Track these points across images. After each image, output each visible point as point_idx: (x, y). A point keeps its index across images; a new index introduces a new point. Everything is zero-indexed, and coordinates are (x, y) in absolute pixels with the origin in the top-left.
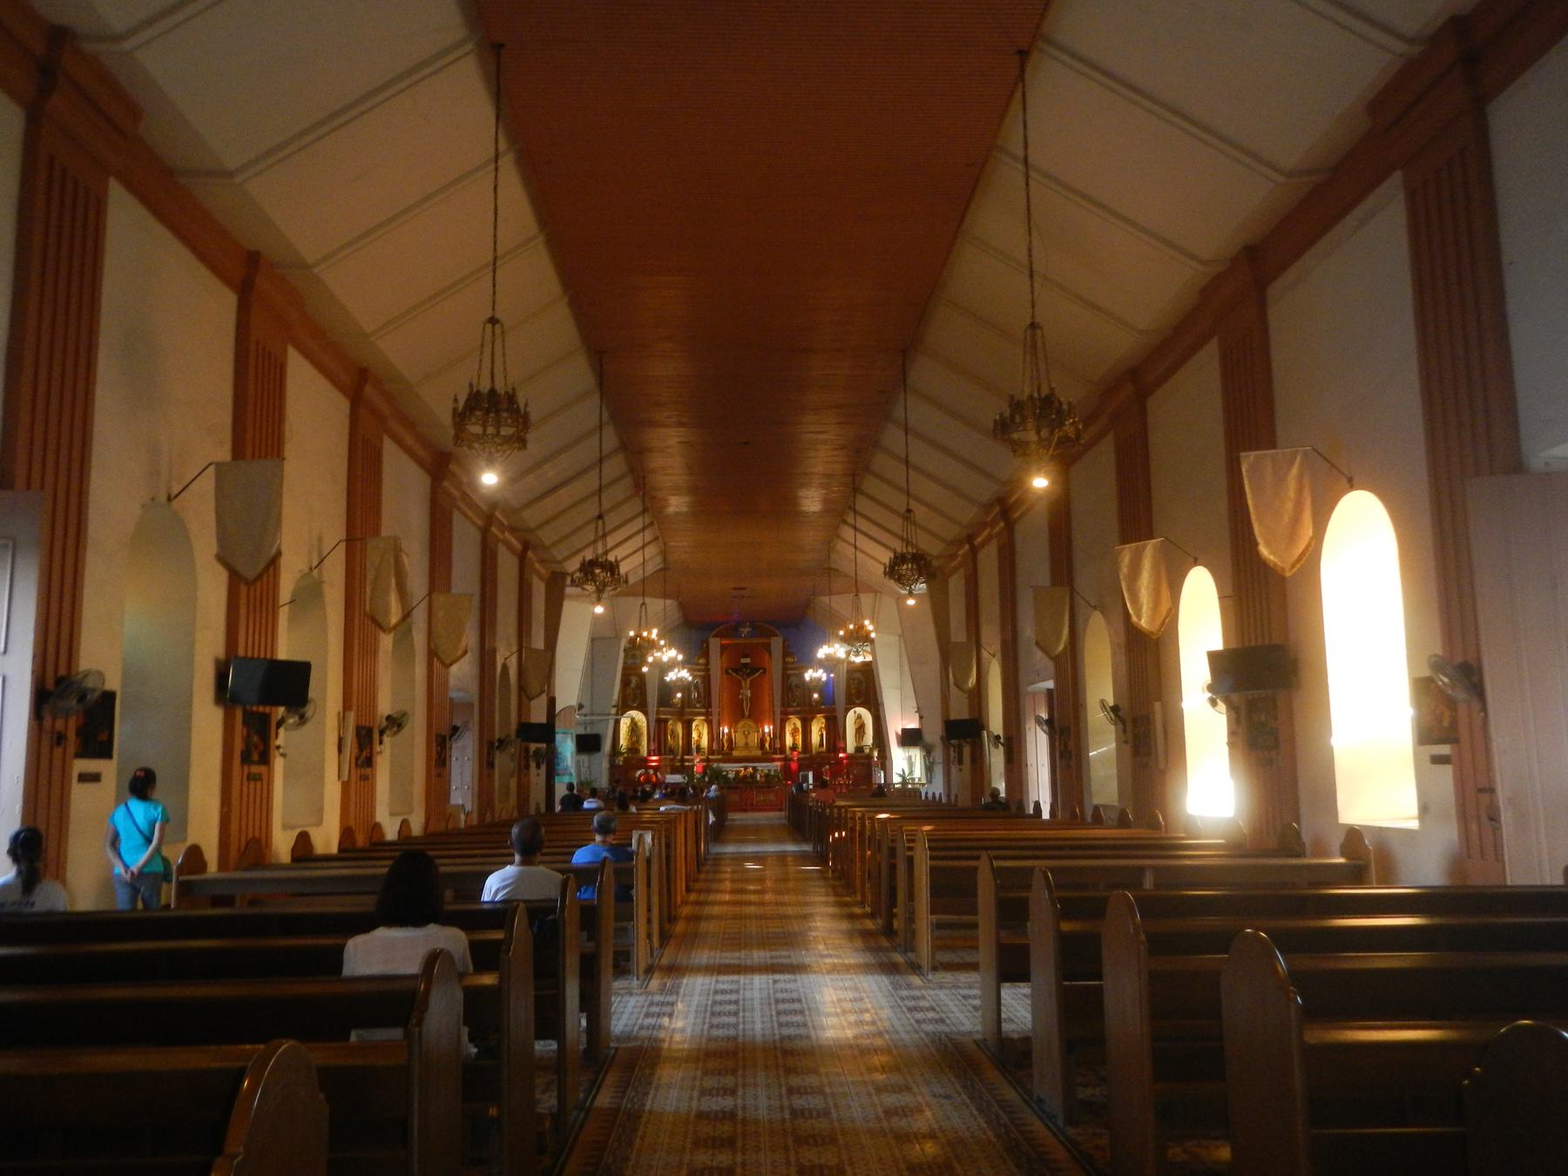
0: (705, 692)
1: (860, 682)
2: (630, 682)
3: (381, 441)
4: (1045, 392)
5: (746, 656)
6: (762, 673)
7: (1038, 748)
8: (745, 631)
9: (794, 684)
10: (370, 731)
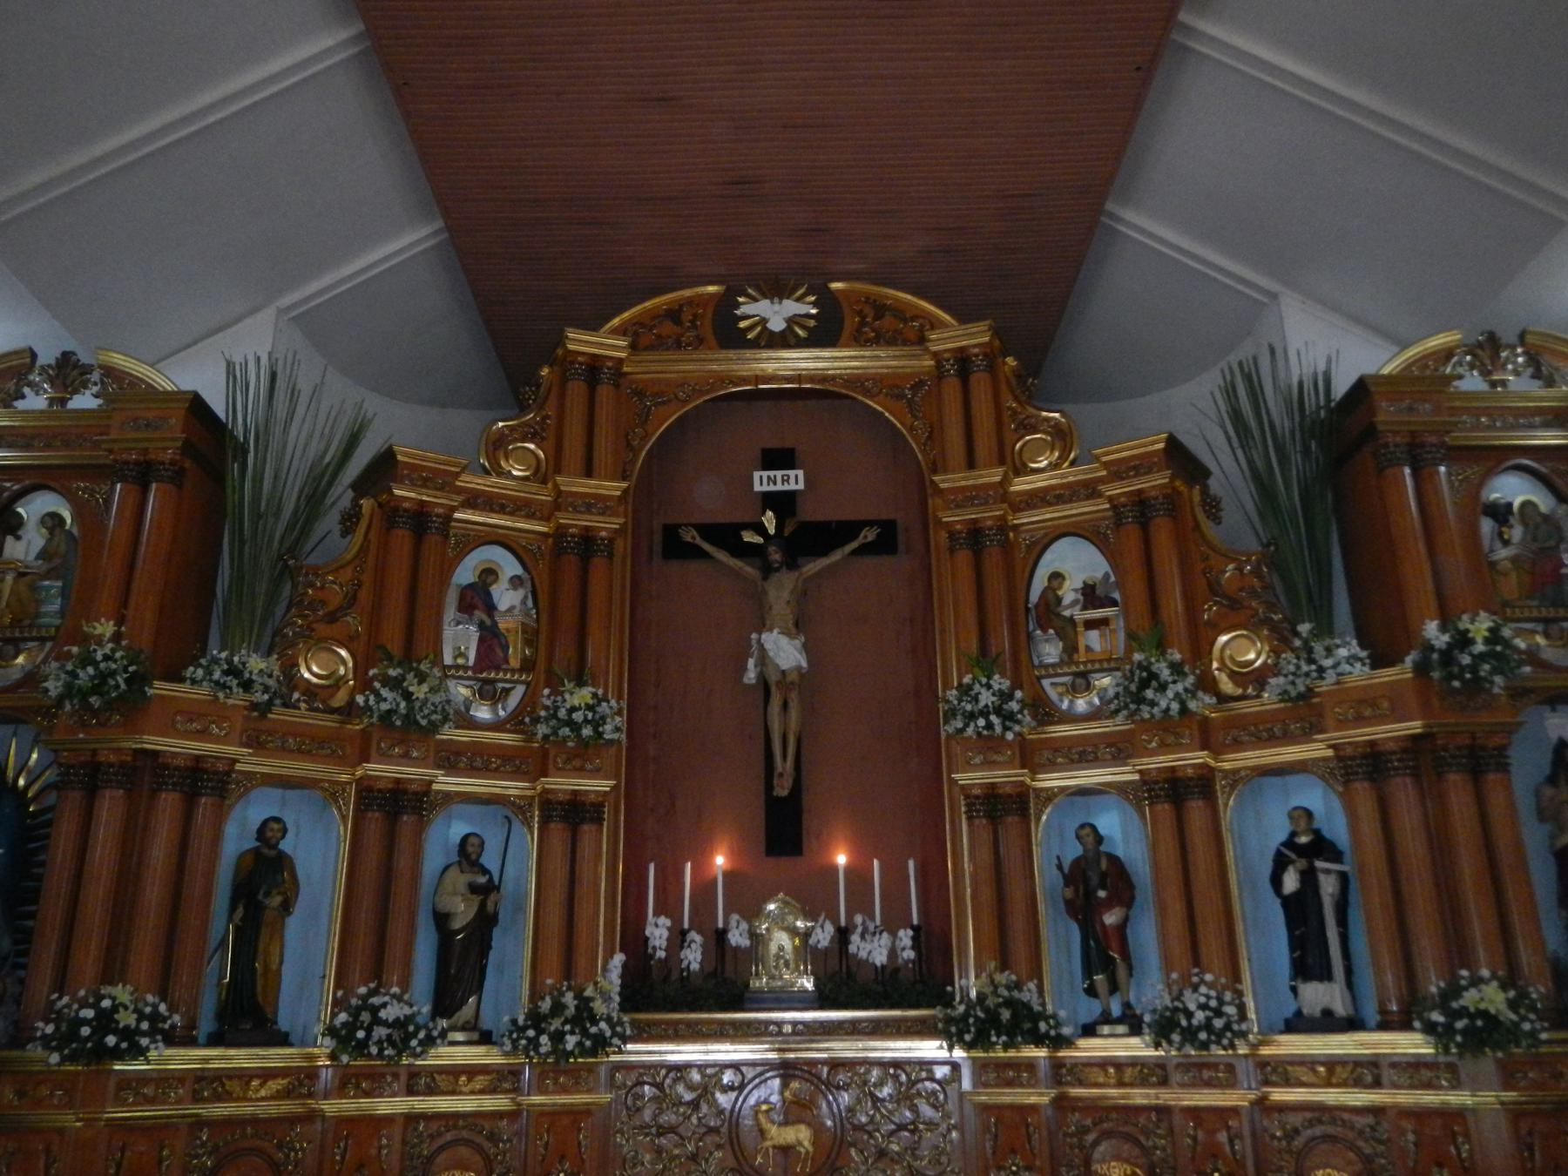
5: (778, 459)
6: (864, 550)
9: (1069, 593)
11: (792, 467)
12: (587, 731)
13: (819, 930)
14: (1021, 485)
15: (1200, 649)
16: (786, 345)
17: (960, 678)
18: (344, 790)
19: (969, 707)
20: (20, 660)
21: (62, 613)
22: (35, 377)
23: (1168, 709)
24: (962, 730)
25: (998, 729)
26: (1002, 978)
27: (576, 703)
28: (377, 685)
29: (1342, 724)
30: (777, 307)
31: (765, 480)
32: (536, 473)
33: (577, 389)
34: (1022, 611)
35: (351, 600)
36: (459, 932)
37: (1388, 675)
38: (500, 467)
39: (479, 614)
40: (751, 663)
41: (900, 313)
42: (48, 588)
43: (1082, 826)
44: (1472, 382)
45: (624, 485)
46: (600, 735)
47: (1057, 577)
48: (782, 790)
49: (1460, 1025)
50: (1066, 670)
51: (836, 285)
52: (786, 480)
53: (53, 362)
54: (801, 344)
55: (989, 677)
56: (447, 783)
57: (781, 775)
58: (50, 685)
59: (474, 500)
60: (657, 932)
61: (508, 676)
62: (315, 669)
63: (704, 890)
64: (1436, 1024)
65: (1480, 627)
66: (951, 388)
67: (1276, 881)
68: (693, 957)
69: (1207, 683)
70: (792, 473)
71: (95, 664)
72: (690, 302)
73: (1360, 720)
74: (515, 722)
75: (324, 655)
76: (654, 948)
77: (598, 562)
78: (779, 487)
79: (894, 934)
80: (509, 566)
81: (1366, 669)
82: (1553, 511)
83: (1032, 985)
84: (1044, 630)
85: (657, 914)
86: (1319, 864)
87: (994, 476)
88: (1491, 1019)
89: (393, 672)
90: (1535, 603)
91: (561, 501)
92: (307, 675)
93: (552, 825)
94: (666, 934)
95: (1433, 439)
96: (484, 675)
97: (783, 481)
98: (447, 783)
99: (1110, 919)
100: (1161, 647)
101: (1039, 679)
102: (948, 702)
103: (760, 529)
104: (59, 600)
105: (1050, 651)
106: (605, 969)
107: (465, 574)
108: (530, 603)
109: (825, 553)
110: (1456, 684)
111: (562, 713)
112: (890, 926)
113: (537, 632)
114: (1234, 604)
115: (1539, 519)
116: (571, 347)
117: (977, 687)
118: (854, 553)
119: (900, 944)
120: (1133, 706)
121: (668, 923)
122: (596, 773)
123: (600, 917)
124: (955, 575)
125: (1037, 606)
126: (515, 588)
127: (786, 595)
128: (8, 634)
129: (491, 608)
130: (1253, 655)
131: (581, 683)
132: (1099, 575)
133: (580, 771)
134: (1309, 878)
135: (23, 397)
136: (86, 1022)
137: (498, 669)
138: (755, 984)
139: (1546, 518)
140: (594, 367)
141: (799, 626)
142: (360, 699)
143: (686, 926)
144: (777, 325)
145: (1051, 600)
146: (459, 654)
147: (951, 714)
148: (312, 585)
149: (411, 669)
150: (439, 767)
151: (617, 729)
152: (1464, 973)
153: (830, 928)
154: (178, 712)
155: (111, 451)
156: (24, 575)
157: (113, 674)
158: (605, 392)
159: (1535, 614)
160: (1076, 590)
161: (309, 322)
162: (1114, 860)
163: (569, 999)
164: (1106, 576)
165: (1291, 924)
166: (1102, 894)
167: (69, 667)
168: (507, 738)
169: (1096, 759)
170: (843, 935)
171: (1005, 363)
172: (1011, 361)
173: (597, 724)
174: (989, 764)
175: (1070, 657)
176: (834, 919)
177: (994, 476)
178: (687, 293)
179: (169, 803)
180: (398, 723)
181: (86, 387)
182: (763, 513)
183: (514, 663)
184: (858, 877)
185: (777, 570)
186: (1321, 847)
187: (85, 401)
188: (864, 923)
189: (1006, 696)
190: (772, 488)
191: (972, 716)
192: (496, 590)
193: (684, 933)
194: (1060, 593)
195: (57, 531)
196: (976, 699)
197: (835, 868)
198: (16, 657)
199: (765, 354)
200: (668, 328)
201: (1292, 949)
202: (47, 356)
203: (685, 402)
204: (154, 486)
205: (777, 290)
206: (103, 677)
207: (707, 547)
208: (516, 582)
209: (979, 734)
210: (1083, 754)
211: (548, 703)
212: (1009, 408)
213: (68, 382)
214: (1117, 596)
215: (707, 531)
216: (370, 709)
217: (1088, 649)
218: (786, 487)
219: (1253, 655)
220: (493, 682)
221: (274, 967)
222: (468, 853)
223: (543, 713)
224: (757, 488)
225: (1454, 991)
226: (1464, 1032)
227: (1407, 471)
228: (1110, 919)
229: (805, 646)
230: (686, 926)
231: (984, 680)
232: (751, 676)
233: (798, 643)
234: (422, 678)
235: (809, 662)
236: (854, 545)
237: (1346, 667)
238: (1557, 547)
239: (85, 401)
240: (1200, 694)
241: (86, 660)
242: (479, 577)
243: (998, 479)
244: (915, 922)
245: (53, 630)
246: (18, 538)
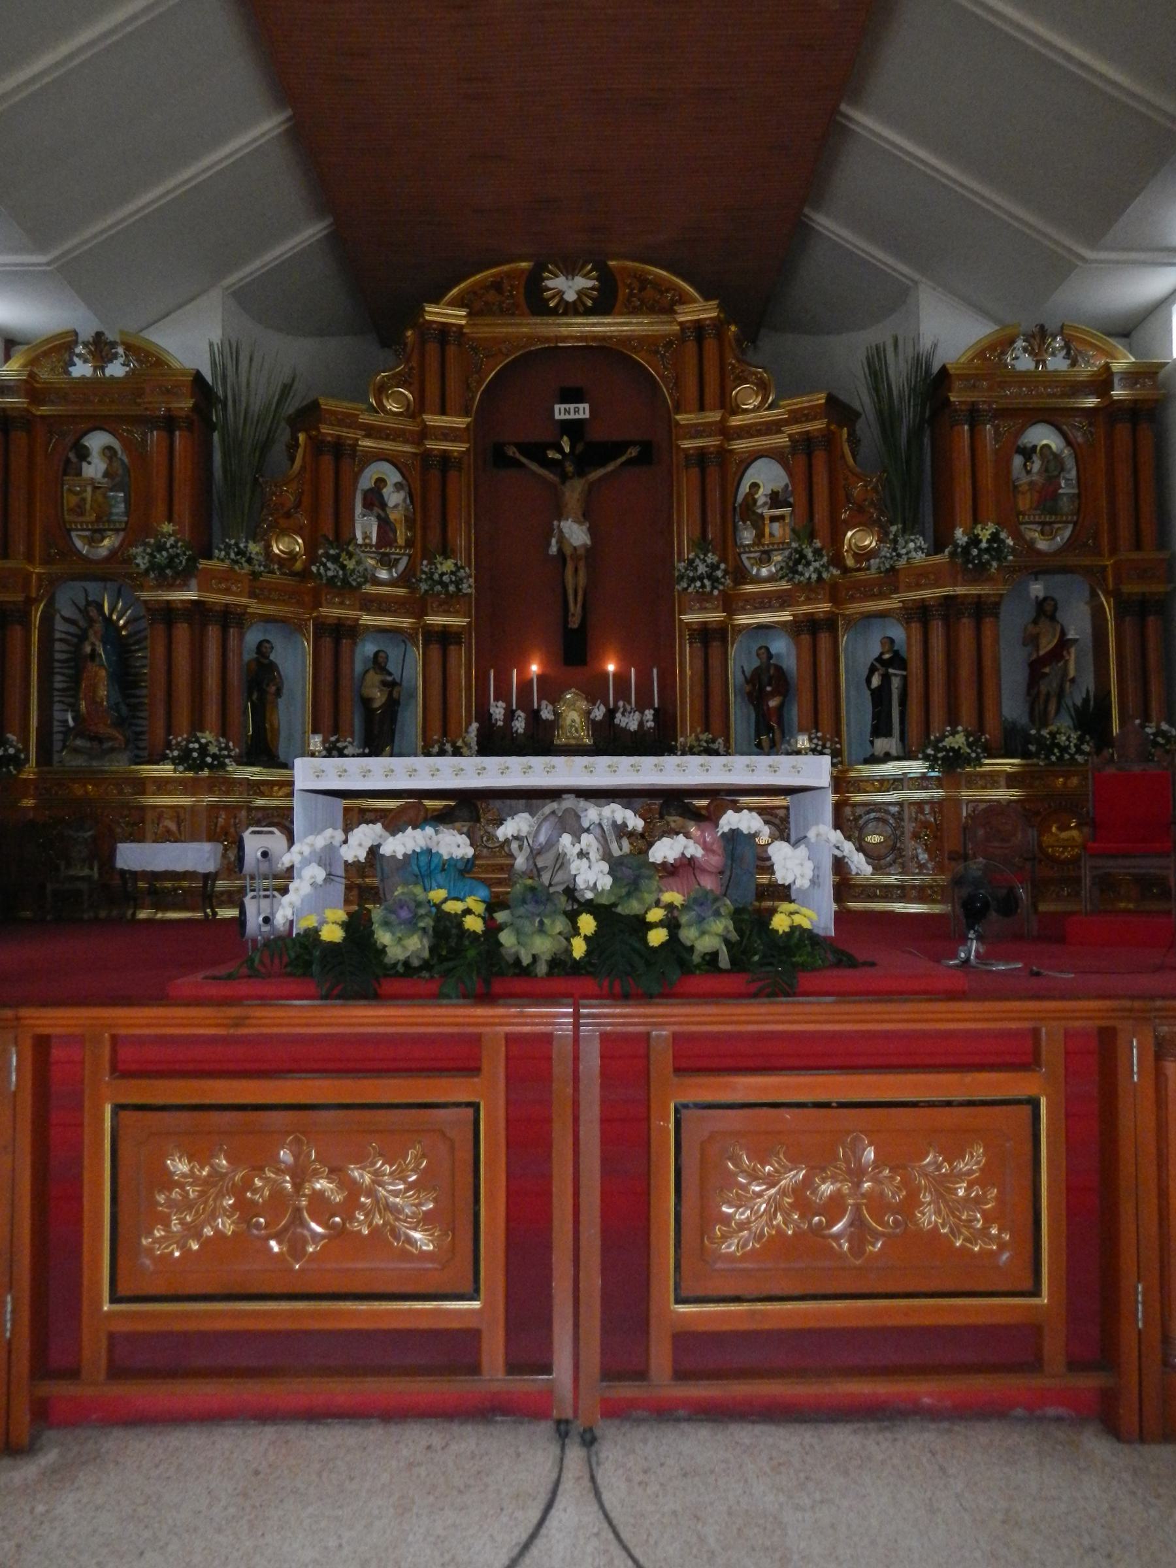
0: (410, 523)
2: (83, 454)
5: (572, 395)
6: (630, 462)
9: (761, 496)
11: (581, 402)
12: (452, 588)
13: (596, 710)
14: (736, 421)
15: (836, 538)
16: (577, 313)
17: (688, 554)
18: (306, 624)
19: (691, 574)
20: (106, 542)
21: (127, 513)
22: (80, 349)
23: (810, 578)
24: (686, 589)
25: (708, 589)
26: (704, 737)
27: (445, 570)
28: (324, 560)
29: (909, 588)
30: (570, 283)
31: (562, 411)
32: (407, 410)
33: (432, 348)
34: (730, 508)
35: (298, 504)
36: (378, 709)
37: (937, 559)
38: (384, 407)
39: (377, 510)
40: (554, 541)
41: (659, 286)
42: (114, 497)
43: (760, 648)
44: (1025, 363)
45: (469, 420)
46: (459, 590)
47: (755, 486)
48: (574, 623)
49: (940, 755)
50: (756, 548)
51: (612, 263)
52: (577, 411)
53: (91, 340)
54: (589, 312)
55: (705, 555)
56: (368, 619)
57: (573, 615)
58: (139, 561)
59: (371, 432)
60: (497, 711)
61: (398, 551)
62: (281, 547)
63: (525, 686)
64: (930, 755)
65: (985, 534)
66: (691, 347)
67: (868, 681)
68: (519, 725)
69: (837, 560)
70: (581, 406)
71: (167, 550)
72: (508, 275)
73: (919, 586)
74: (404, 580)
75: (286, 539)
76: (496, 720)
77: (453, 474)
78: (572, 416)
79: (642, 713)
80: (393, 476)
81: (923, 556)
82: (1062, 452)
83: (720, 740)
84: (744, 522)
85: (496, 699)
86: (891, 671)
87: (714, 416)
88: (957, 752)
89: (332, 552)
90: (1039, 512)
91: (425, 432)
92: (277, 551)
93: (431, 646)
94: (503, 711)
95: (985, 407)
96: (383, 550)
97: (575, 412)
98: (368, 619)
99: (773, 703)
100: (812, 536)
101: (739, 554)
102: (679, 570)
103: (560, 450)
104: (123, 505)
105: (747, 536)
106: (467, 732)
107: (366, 481)
108: (408, 501)
109: (603, 464)
110: (970, 566)
111: (436, 577)
112: (641, 709)
113: (414, 521)
114: (860, 510)
115: (1051, 457)
116: (428, 318)
117: (697, 560)
118: (623, 464)
119: (645, 718)
120: (790, 575)
121: (504, 705)
122: (456, 614)
123: (462, 703)
124: (687, 484)
125: (740, 505)
126: (398, 491)
127: (576, 496)
128: (96, 527)
129: (383, 505)
130: (870, 541)
131: (446, 558)
132: (782, 484)
133: (447, 613)
134: (886, 678)
135: (75, 365)
136: (194, 750)
137: (390, 545)
138: (557, 742)
139: (1057, 457)
140: (444, 330)
141: (587, 515)
142: (314, 569)
143: (514, 707)
144: (571, 296)
145: (750, 499)
146: (366, 536)
147: (681, 577)
148: (274, 494)
149: (343, 550)
150: (361, 610)
151: (470, 586)
152: (948, 728)
153: (603, 709)
154: (214, 578)
155: (146, 409)
156: (99, 488)
157: (177, 555)
158: (452, 350)
159: (1037, 519)
160: (766, 495)
161: (242, 297)
162: (779, 669)
163: (448, 747)
164: (787, 486)
165: (875, 705)
166: (769, 689)
167: (149, 550)
168: (400, 591)
169: (770, 606)
170: (611, 713)
171: (729, 329)
172: (733, 328)
173: (458, 583)
174: (703, 609)
175: (759, 540)
176: (606, 704)
177: (714, 416)
178: (505, 268)
179: (213, 632)
180: (339, 584)
181: (116, 358)
182: (562, 438)
183: (401, 541)
184: (621, 678)
185: (571, 478)
186: (898, 660)
187: (116, 369)
188: (624, 706)
189: (714, 567)
190: (567, 417)
191: (692, 580)
192: (386, 491)
193: (513, 712)
194: (756, 496)
195: (114, 459)
196: (696, 569)
197: (605, 674)
198: (102, 540)
199: (564, 320)
200: (492, 296)
201: (873, 719)
202: (86, 334)
203: (507, 356)
204: (177, 433)
205: (570, 270)
206: (171, 559)
207: (524, 460)
208: (398, 487)
209: (697, 591)
210: (763, 603)
211: (426, 569)
212: (731, 364)
213: (104, 354)
214: (791, 500)
215: (525, 449)
216: (320, 574)
217: (771, 535)
218: (577, 416)
219: (870, 541)
220: (387, 555)
221: (276, 726)
222: (378, 663)
223: (424, 576)
224: (557, 417)
225: (942, 738)
226: (943, 758)
227: (966, 427)
228: (773, 703)
229: (589, 529)
230: (514, 707)
231: (702, 557)
232: (553, 549)
233: (585, 528)
234: (350, 556)
235: (592, 539)
236: (623, 459)
237: (913, 554)
238: (1058, 476)
239: (116, 369)
240: (831, 568)
241: (160, 547)
242: (375, 483)
243: (718, 419)
244: (656, 706)
245: (123, 526)
246: (89, 463)
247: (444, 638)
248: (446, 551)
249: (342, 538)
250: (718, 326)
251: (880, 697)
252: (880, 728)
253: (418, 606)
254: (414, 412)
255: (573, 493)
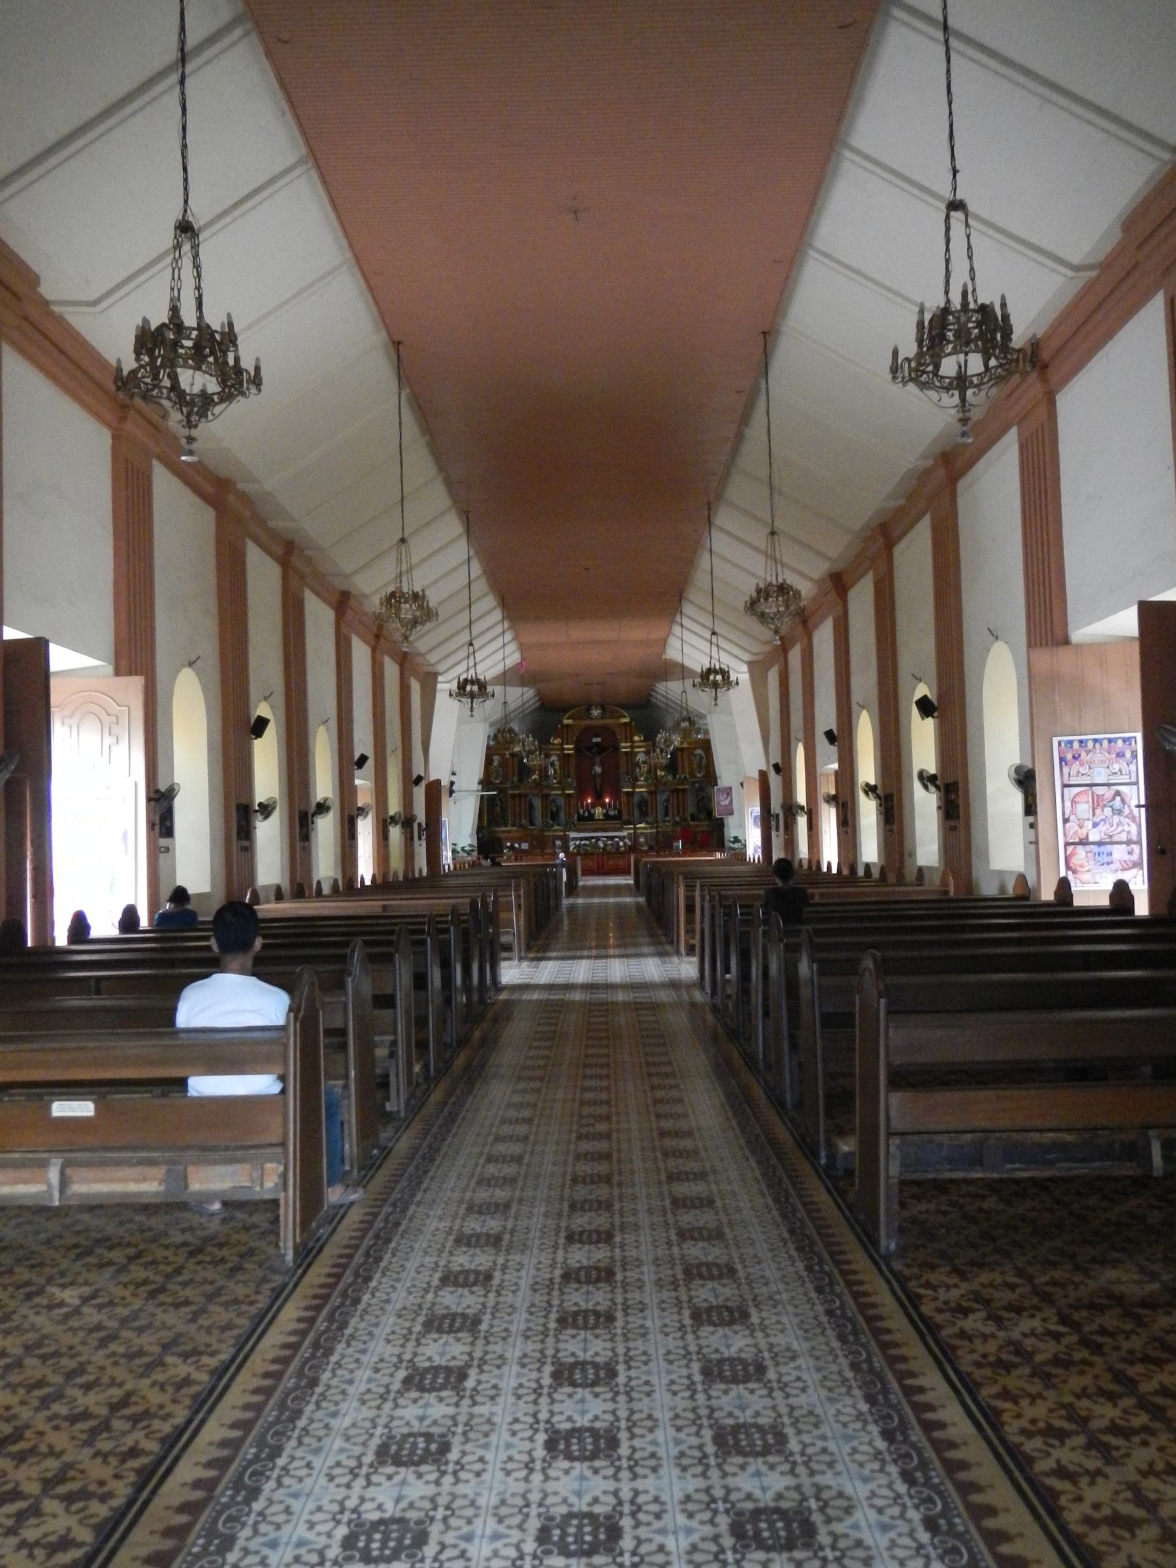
1: (701, 758)
3: (303, 591)
4: (780, 580)
5: (597, 736)
7: (829, 820)
8: (596, 713)
10: (306, 814)
74: (560, 782)
91: (563, 749)
140: (568, 726)
141: (602, 765)
184: (610, 804)
210: (641, 787)
247: (569, 795)
248: (569, 776)
249: (547, 777)
250: (630, 723)
251: (666, 808)
252: (667, 815)
253: (563, 789)
254: (562, 744)
255: (598, 759)
